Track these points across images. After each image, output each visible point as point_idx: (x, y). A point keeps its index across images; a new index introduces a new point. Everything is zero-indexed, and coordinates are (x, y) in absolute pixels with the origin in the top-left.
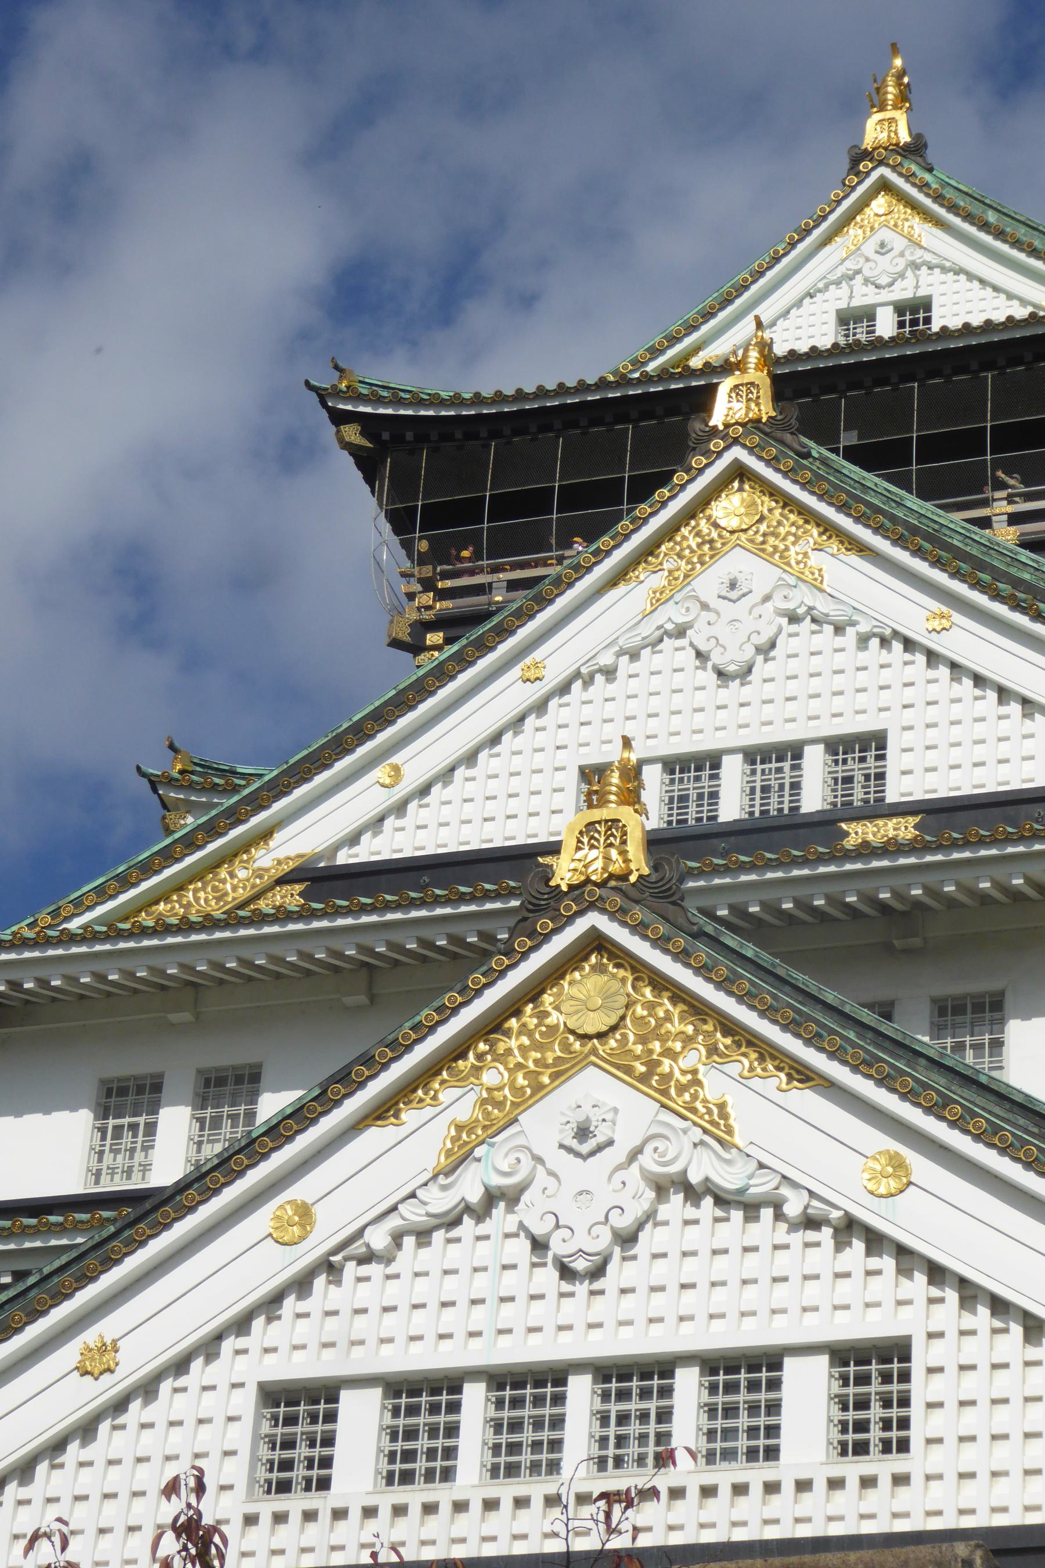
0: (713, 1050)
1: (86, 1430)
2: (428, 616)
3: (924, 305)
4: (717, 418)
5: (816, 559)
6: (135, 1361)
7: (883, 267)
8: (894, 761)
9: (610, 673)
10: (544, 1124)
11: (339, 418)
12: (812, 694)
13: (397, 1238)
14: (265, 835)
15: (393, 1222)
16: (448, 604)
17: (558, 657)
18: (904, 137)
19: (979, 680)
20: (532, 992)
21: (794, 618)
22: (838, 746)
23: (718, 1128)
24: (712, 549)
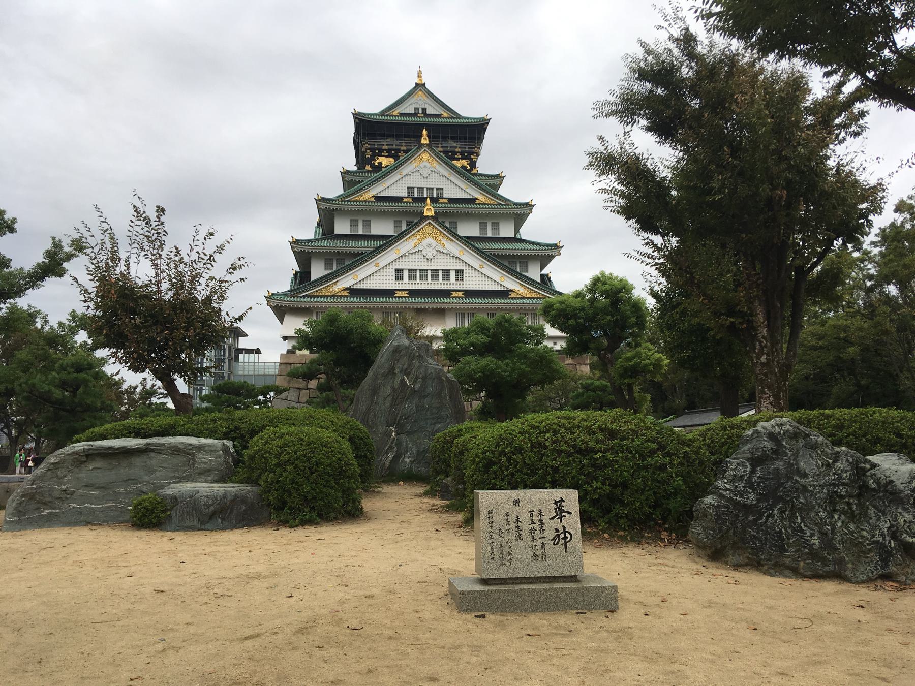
7: (420, 102)
10: (425, 242)
17: (404, 172)
23: (443, 245)
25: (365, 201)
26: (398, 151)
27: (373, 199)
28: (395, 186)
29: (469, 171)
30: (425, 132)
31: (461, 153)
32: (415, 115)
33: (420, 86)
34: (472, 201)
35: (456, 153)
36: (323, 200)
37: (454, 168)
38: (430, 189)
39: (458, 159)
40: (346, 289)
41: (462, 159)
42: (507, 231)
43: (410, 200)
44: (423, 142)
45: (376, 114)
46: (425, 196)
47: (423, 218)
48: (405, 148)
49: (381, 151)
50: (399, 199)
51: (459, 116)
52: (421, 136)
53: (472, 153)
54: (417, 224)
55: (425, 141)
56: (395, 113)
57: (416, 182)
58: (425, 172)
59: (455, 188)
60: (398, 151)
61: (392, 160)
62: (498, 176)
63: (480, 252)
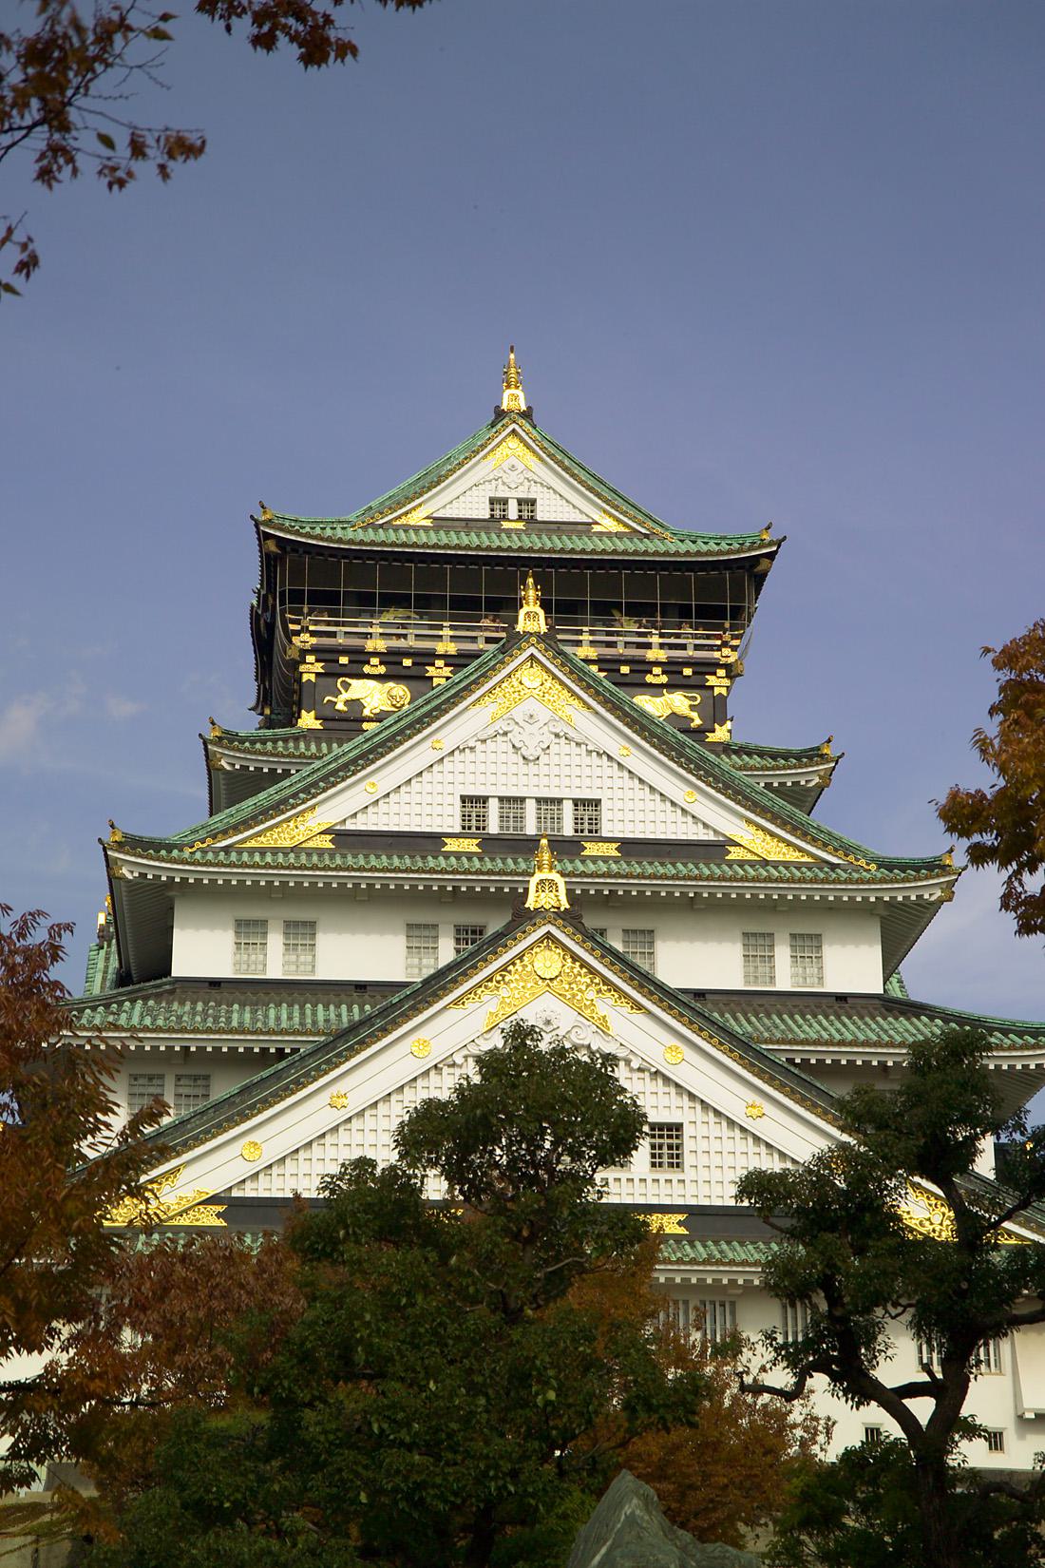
0: (599, 991)
1: (335, 1129)
2: (308, 646)
3: (533, 502)
4: (520, 628)
5: (569, 710)
6: (355, 1104)
7: (513, 478)
8: (605, 814)
9: (472, 749)
11: (268, 536)
12: (568, 776)
13: (466, 1057)
14: (313, 808)
15: (465, 1052)
16: (314, 640)
18: (524, 408)
19: (641, 781)
20: (521, 956)
21: (557, 735)
22: (576, 802)
23: (603, 1028)
25: (295, 849)
26: (430, 657)
27: (325, 842)
28: (412, 792)
29: (699, 733)
31: (671, 667)
32: (494, 522)
34: (715, 849)
35: (642, 666)
36: (134, 844)
37: (640, 723)
39: (656, 689)
40: (213, 1200)
41: (671, 687)
42: (852, 965)
43: (471, 846)
46: (531, 829)
47: (522, 917)
48: (452, 648)
49: (360, 657)
52: (515, 604)
53: (712, 666)
54: (500, 940)
55: (531, 618)
56: (417, 518)
57: (495, 775)
58: (531, 740)
59: (650, 802)
60: (430, 657)
61: (400, 690)
62: (813, 755)
63: (750, 1054)
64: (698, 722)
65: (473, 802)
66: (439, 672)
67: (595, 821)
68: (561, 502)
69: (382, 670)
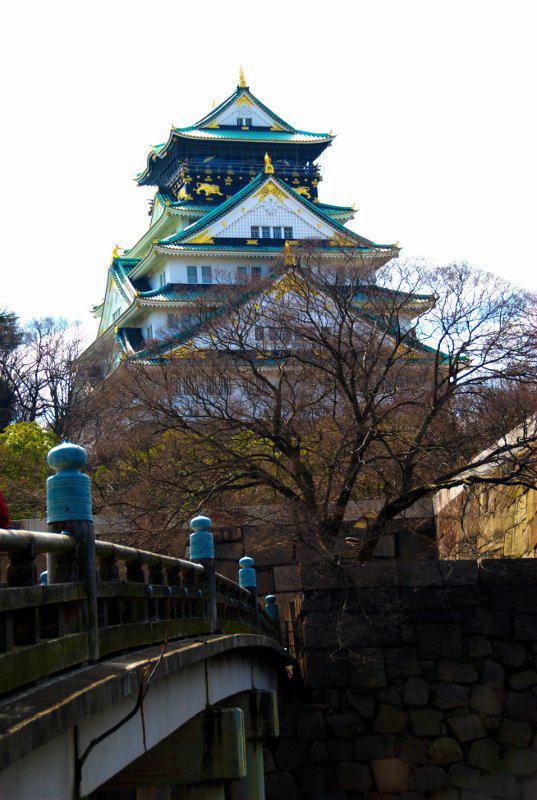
11: (174, 136)
24: (266, 192)
26: (226, 176)
27: (212, 242)
30: (267, 157)
32: (237, 128)
33: (242, 90)
34: (324, 244)
37: (295, 195)
38: (277, 229)
43: (255, 242)
44: (267, 171)
45: (193, 128)
50: (239, 243)
51: (293, 132)
55: (269, 168)
59: (308, 227)
62: (349, 210)
64: (309, 197)
65: (254, 229)
66: (228, 181)
67: (291, 234)
68: (262, 120)
69: (211, 180)
